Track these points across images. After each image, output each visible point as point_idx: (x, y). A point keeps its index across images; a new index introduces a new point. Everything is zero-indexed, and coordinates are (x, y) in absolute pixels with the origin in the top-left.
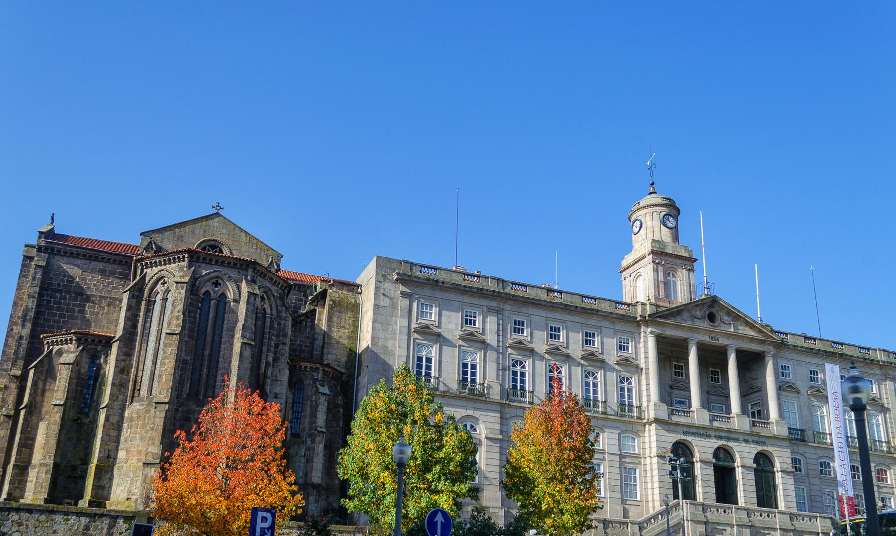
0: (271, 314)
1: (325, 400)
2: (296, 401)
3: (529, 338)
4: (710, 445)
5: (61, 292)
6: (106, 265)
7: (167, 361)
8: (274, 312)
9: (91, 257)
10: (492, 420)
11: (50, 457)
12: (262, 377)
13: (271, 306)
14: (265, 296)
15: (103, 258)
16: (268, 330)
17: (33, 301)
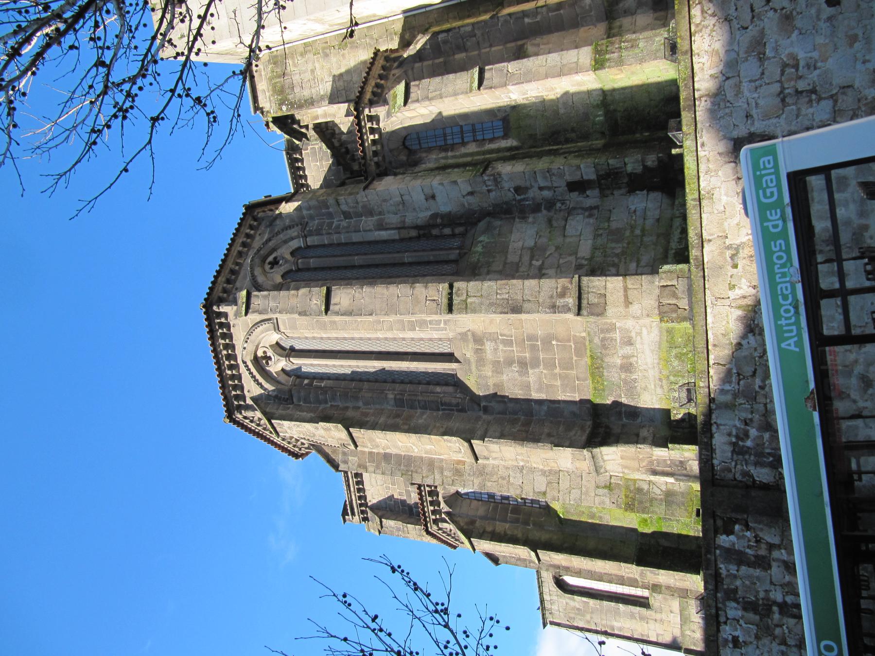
0: (298, 237)
1: (418, 86)
2: (442, 143)
7: (400, 444)
8: (293, 232)
11: (628, 568)
12: (405, 234)
13: (285, 242)
14: (271, 259)
16: (325, 237)
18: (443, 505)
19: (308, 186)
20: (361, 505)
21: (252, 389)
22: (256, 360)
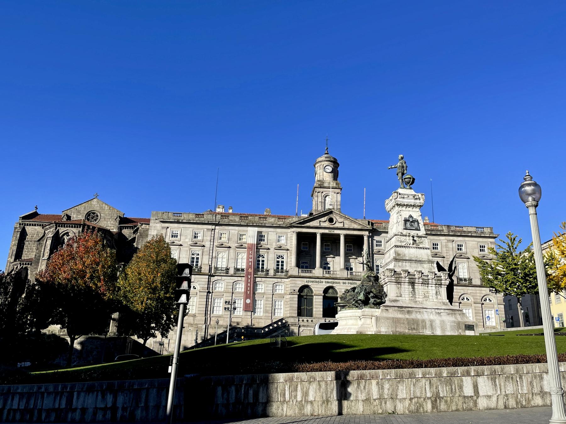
3: (228, 241)
4: (321, 286)
10: (204, 283)
18: (25, 266)
19: (123, 229)
20: (25, 224)
21: (62, 230)
22: (68, 233)
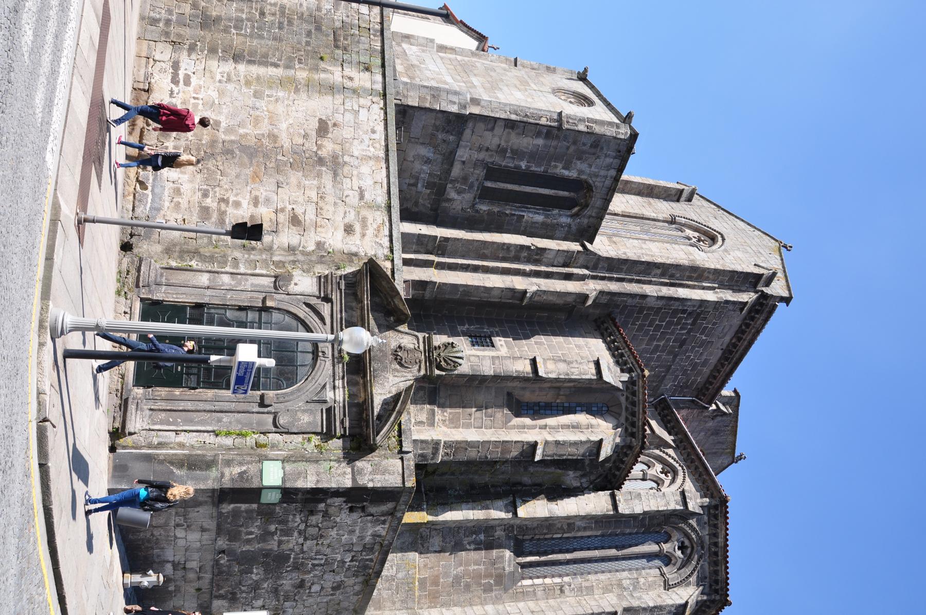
5: (693, 324)
6: (711, 367)
9: (731, 352)
15: (723, 365)
17: (694, 306)
